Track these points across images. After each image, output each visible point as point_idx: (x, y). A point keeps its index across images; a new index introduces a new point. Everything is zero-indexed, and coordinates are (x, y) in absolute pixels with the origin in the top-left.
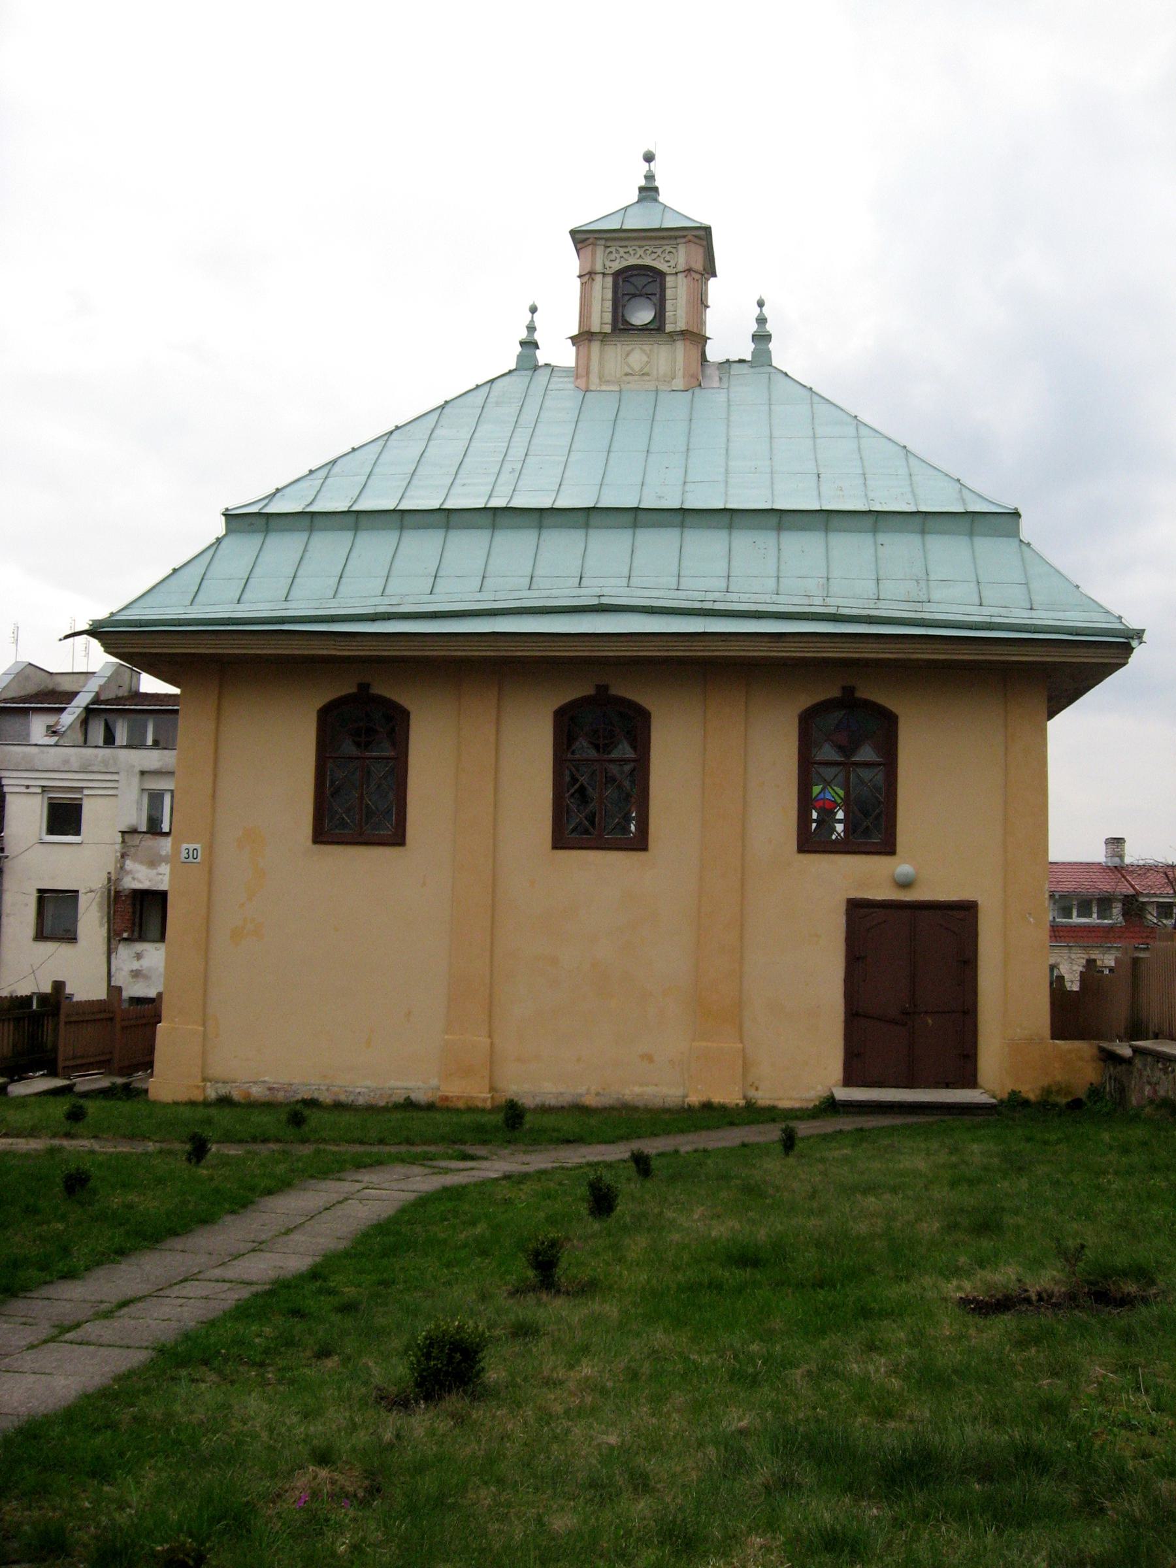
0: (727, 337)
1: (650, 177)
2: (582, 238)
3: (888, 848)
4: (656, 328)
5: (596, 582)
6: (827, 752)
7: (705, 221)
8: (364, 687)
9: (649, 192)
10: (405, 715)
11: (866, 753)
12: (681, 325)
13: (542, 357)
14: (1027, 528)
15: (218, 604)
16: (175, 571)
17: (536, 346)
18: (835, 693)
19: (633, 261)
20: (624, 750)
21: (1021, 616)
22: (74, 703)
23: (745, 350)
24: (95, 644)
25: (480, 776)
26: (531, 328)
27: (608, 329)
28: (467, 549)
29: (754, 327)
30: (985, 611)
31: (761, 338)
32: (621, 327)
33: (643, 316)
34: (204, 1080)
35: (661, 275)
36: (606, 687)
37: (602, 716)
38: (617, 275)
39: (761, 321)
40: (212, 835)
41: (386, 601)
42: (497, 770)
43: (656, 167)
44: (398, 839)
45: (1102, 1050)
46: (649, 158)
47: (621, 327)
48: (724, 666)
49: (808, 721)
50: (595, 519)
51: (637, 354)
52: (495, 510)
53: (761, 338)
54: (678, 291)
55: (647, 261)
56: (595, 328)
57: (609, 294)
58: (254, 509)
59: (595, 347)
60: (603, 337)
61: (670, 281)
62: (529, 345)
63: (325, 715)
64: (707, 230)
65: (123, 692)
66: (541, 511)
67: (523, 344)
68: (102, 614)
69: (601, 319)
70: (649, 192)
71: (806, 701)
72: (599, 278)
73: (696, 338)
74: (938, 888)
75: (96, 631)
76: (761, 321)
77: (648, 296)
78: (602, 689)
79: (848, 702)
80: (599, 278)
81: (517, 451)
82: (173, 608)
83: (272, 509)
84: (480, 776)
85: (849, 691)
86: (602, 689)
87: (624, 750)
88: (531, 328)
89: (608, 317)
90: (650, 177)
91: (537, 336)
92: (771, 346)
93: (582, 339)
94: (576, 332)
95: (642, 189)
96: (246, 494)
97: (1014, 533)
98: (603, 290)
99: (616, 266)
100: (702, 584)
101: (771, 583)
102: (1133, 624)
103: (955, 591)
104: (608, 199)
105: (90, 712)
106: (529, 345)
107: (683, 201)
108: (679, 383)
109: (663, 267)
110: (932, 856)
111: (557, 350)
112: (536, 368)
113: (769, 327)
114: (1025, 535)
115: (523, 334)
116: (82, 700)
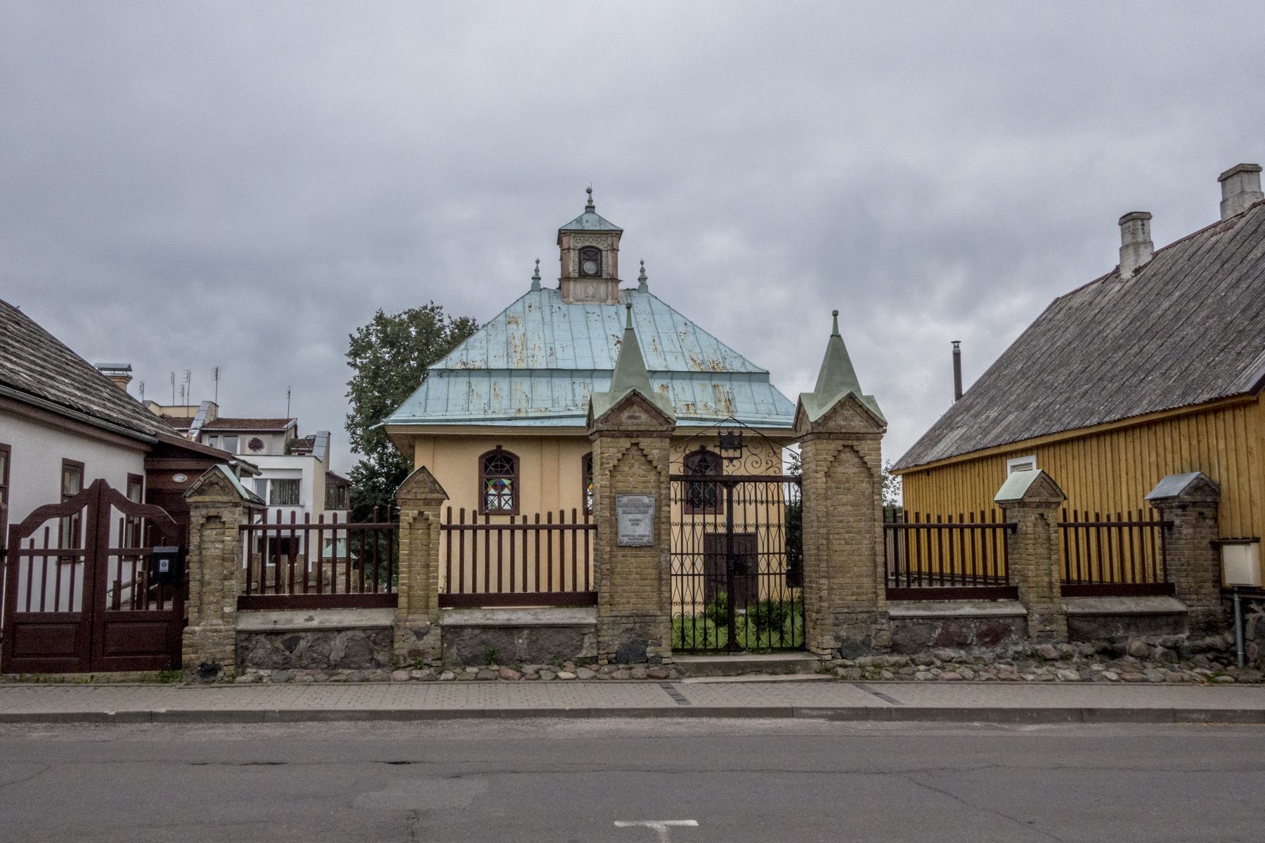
0: (628, 278)
1: (590, 201)
4: (597, 276)
8: (499, 447)
9: (590, 208)
10: (517, 458)
13: (543, 284)
19: (587, 244)
22: (193, 425)
23: (636, 285)
26: (537, 271)
27: (577, 275)
28: (542, 388)
29: (639, 274)
31: (642, 279)
32: (583, 275)
33: (590, 267)
35: (600, 251)
38: (580, 250)
39: (642, 271)
46: (589, 191)
50: (595, 374)
51: (590, 288)
52: (552, 370)
53: (642, 279)
54: (607, 258)
55: (594, 244)
59: (572, 284)
60: (575, 279)
61: (604, 253)
62: (536, 278)
63: (481, 458)
69: (572, 268)
70: (590, 208)
73: (614, 280)
76: (642, 271)
79: (703, 451)
85: (703, 448)
88: (537, 271)
90: (590, 201)
91: (540, 274)
92: (648, 282)
93: (565, 278)
97: (768, 381)
98: (574, 256)
99: (580, 246)
104: (570, 212)
106: (536, 278)
113: (646, 273)
114: (772, 382)
116: (197, 424)
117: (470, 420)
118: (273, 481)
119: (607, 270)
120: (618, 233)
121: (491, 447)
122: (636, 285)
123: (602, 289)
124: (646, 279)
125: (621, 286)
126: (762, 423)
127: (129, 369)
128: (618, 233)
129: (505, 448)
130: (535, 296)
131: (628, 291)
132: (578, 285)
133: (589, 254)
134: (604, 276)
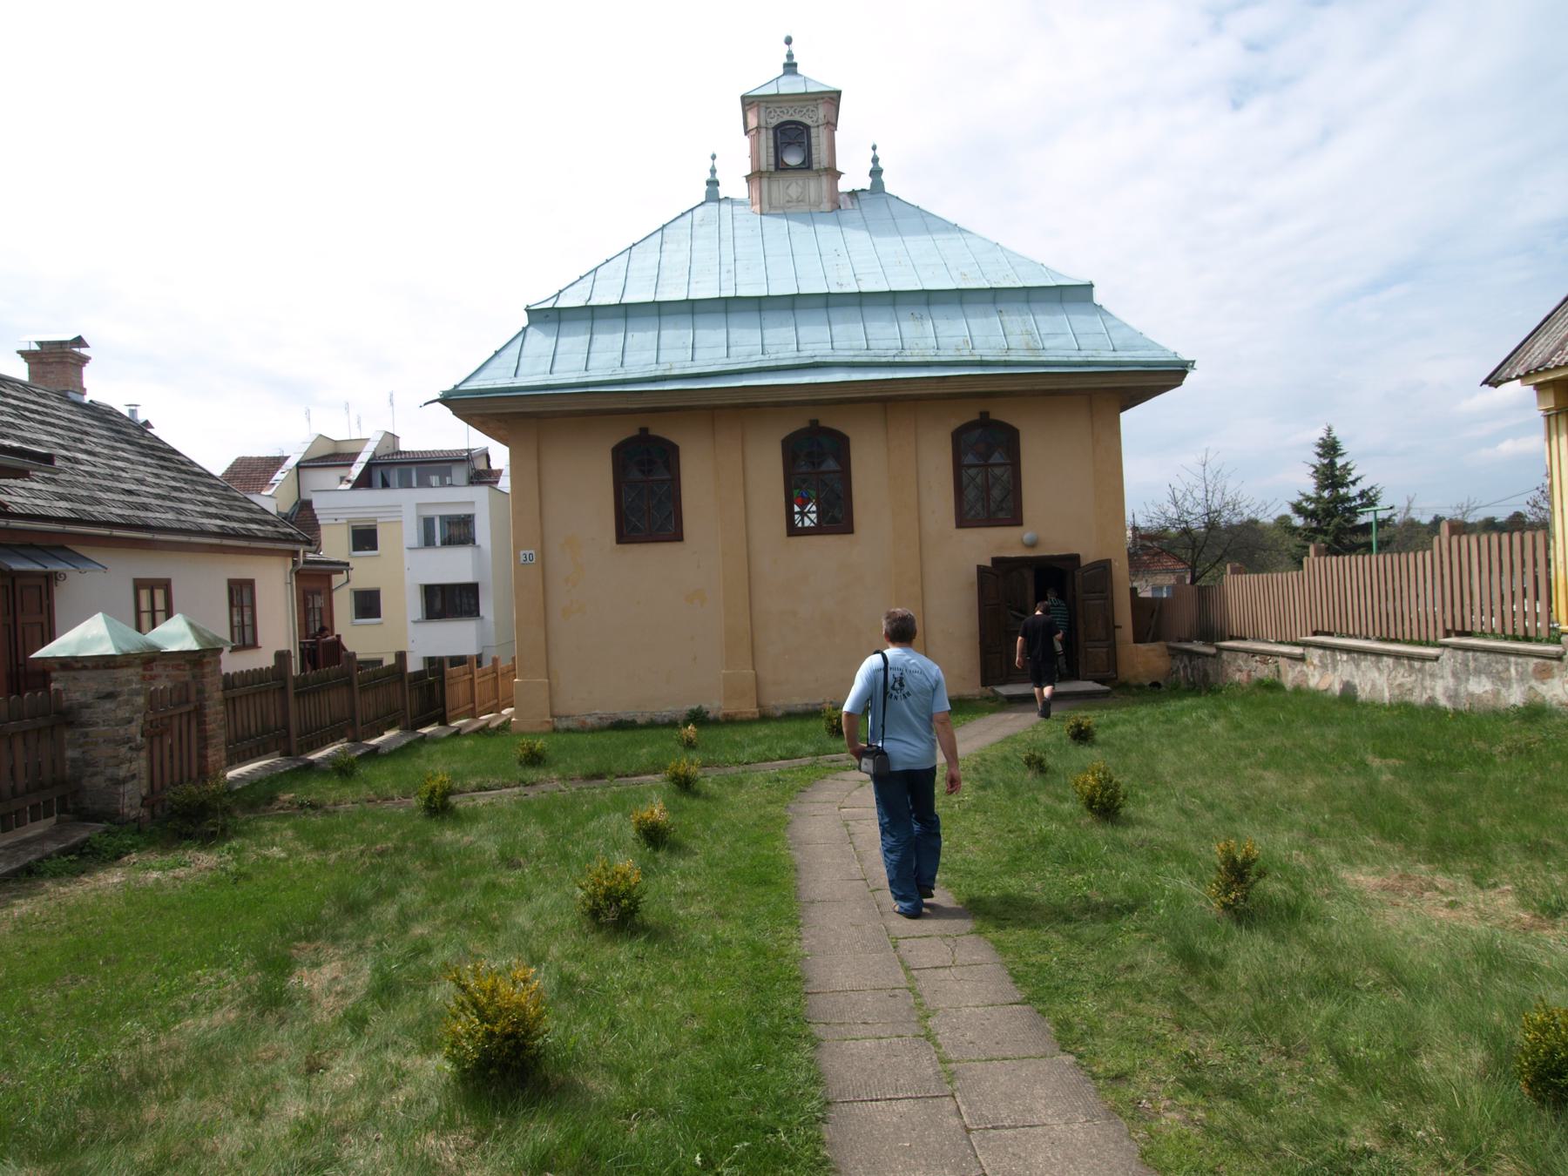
1: (790, 56)
2: (748, 102)
3: (1016, 520)
4: (806, 165)
5: (809, 346)
6: (969, 459)
7: (838, 88)
9: (790, 67)
10: (674, 449)
11: (996, 458)
12: (825, 164)
14: (1098, 296)
15: (534, 375)
16: (497, 353)
17: (717, 183)
18: (975, 417)
19: (786, 118)
20: (831, 465)
21: (1107, 356)
23: (866, 183)
24: (446, 412)
25: (734, 491)
26: (713, 171)
27: (772, 168)
29: (871, 166)
30: (1083, 353)
31: (876, 173)
32: (780, 167)
33: (793, 159)
34: (552, 716)
35: (808, 128)
36: (987, 414)
37: (815, 442)
38: (776, 128)
39: (875, 160)
40: (542, 542)
41: (662, 367)
42: (745, 485)
43: (794, 47)
44: (678, 537)
45: (1169, 648)
47: (780, 167)
48: (896, 401)
49: (957, 436)
51: (793, 187)
53: (876, 173)
54: (819, 138)
55: (797, 118)
56: (764, 168)
57: (771, 144)
58: (549, 305)
59: (765, 182)
61: (813, 132)
62: (713, 183)
64: (839, 93)
65: (390, 450)
66: (759, 298)
67: (708, 183)
68: (449, 387)
69: (767, 160)
70: (790, 67)
71: (956, 423)
72: (763, 131)
74: (1054, 546)
75: (447, 400)
76: (875, 160)
77: (800, 144)
78: (984, 415)
79: (985, 422)
80: (763, 131)
81: (728, 259)
82: (498, 378)
83: (562, 303)
84: (734, 491)
86: (984, 415)
87: (831, 465)
88: (713, 171)
89: (772, 160)
90: (790, 56)
91: (718, 176)
92: (884, 177)
93: (754, 177)
94: (749, 172)
95: (785, 65)
96: (540, 296)
98: (767, 139)
99: (775, 122)
100: (883, 344)
101: (932, 342)
102: (1185, 356)
103: (1059, 341)
104: (763, 75)
105: (370, 466)
106: (713, 183)
107: (817, 74)
108: (826, 206)
109: (808, 122)
110: (1050, 523)
111: (735, 185)
112: (719, 201)
113: (881, 164)
115: (708, 176)
116: (364, 458)
117: (587, 385)
118: (441, 517)
119: (820, 157)
120: (834, 98)
121: (628, 430)
122: (866, 183)
123: (815, 187)
124: (881, 171)
125: (844, 185)
126: (1089, 364)
127: (79, 341)
128: (834, 98)
129: (655, 431)
130: (712, 206)
131: (853, 194)
132: (775, 186)
133: (792, 136)
134: (815, 166)
